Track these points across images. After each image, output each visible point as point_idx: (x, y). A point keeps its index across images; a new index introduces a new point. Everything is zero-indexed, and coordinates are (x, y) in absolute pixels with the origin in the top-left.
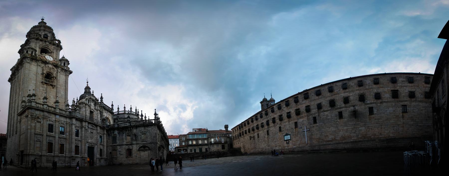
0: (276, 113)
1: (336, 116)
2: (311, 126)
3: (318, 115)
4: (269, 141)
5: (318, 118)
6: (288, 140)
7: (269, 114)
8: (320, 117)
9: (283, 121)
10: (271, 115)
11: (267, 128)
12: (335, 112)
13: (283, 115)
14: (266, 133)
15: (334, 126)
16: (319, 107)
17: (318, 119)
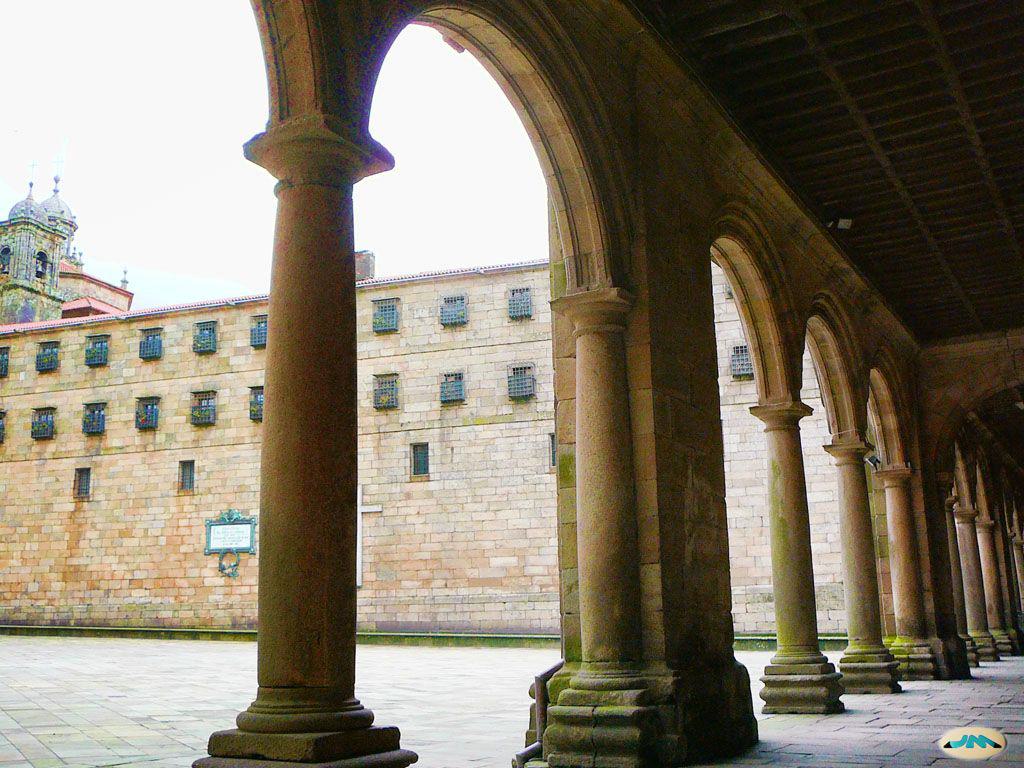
0: (171, 367)
1: (535, 457)
2: (395, 489)
3: (442, 435)
4: (82, 544)
5: (438, 452)
6: (241, 551)
7: (115, 361)
8: (452, 449)
9: (214, 433)
10: (129, 372)
11: (87, 450)
12: (531, 431)
13: (220, 392)
14: (68, 482)
15: (520, 504)
16: (453, 394)
17: (437, 460)
